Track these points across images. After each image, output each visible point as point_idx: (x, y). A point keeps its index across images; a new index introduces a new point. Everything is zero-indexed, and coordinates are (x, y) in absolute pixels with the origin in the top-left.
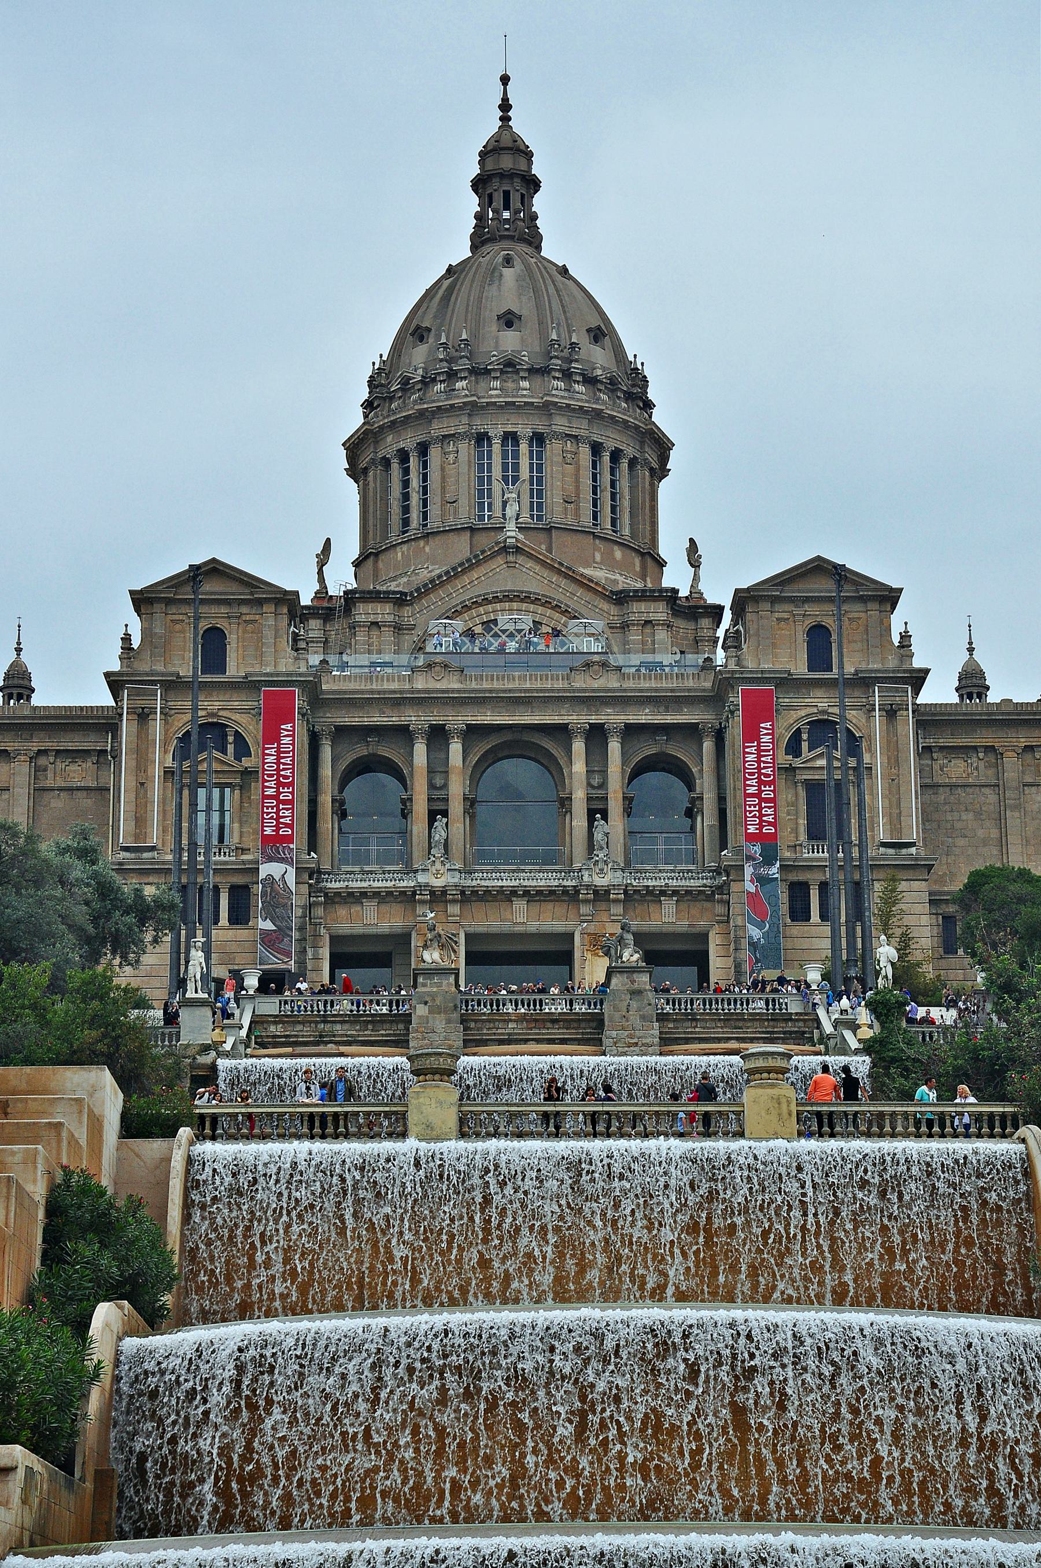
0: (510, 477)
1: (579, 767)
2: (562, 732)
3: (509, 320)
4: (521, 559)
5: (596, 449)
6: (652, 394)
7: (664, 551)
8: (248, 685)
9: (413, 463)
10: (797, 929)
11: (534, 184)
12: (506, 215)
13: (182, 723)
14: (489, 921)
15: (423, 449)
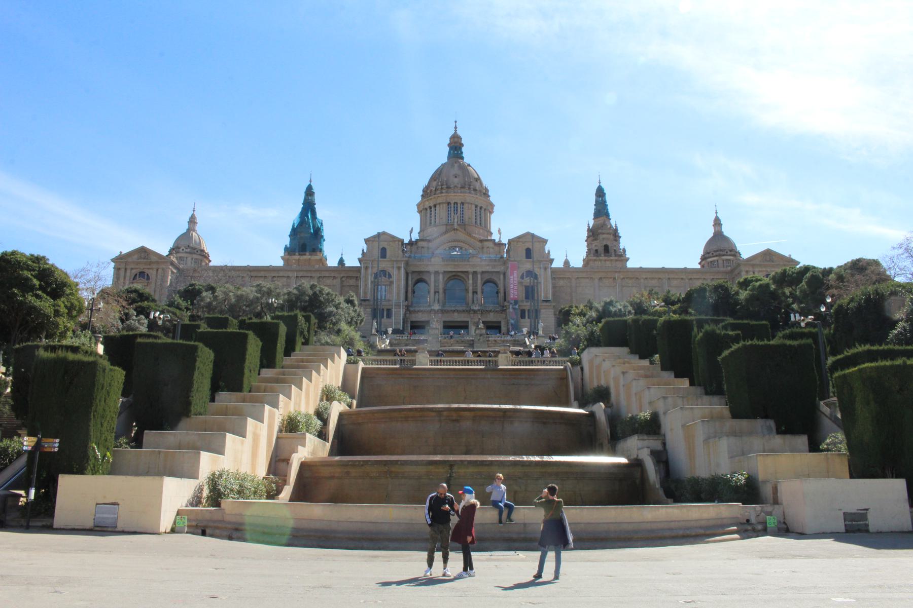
0: (456, 212)
1: (471, 281)
5: (476, 206)
7: (492, 231)
10: (523, 320)
13: (375, 270)
14: (449, 318)
15: (435, 206)
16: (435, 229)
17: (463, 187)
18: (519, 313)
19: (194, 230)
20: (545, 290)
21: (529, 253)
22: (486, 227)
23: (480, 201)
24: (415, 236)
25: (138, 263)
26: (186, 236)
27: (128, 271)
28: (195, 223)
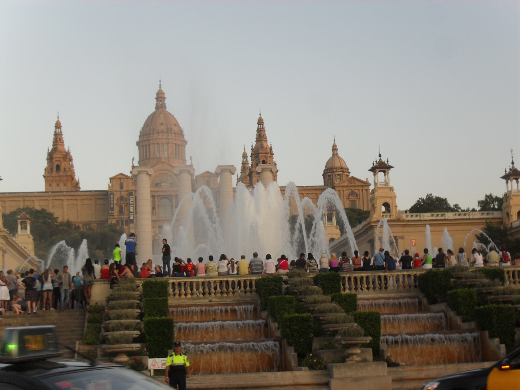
2: (171, 196)
3: (162, 124)
4: (164, 164)
5: (176, 144)
6: (184, 134)
8: (126, 191)
9: (148, 147)
11: (165, 98)
12: (161, 103)
15: (149, 145)
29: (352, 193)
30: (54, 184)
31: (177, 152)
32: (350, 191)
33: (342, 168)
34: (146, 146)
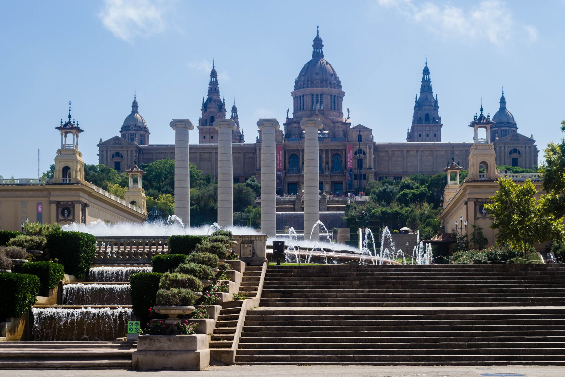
1: (324, 156)
5: (331, 96)
6: (341, 84)
9: (302, 98)
15: (303, 96)
16: (303, 113)
17: (322, 82)
18: (353, 176)
19: (137, 112)
20: (369, 161)
21: (360, 138)
22: (338, 110)
23: (334, 91)
24: (291, 116)
25: (114, 147)
26: (132, 117)
27: (109, 152)
28: (137, 107)
29: (515, 151)
30: (208, 137)
31: (333, 104)
32: (512, 148)
33: (508, 123)
34: (300, 97)
